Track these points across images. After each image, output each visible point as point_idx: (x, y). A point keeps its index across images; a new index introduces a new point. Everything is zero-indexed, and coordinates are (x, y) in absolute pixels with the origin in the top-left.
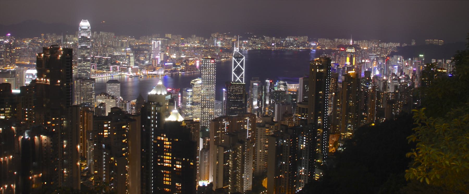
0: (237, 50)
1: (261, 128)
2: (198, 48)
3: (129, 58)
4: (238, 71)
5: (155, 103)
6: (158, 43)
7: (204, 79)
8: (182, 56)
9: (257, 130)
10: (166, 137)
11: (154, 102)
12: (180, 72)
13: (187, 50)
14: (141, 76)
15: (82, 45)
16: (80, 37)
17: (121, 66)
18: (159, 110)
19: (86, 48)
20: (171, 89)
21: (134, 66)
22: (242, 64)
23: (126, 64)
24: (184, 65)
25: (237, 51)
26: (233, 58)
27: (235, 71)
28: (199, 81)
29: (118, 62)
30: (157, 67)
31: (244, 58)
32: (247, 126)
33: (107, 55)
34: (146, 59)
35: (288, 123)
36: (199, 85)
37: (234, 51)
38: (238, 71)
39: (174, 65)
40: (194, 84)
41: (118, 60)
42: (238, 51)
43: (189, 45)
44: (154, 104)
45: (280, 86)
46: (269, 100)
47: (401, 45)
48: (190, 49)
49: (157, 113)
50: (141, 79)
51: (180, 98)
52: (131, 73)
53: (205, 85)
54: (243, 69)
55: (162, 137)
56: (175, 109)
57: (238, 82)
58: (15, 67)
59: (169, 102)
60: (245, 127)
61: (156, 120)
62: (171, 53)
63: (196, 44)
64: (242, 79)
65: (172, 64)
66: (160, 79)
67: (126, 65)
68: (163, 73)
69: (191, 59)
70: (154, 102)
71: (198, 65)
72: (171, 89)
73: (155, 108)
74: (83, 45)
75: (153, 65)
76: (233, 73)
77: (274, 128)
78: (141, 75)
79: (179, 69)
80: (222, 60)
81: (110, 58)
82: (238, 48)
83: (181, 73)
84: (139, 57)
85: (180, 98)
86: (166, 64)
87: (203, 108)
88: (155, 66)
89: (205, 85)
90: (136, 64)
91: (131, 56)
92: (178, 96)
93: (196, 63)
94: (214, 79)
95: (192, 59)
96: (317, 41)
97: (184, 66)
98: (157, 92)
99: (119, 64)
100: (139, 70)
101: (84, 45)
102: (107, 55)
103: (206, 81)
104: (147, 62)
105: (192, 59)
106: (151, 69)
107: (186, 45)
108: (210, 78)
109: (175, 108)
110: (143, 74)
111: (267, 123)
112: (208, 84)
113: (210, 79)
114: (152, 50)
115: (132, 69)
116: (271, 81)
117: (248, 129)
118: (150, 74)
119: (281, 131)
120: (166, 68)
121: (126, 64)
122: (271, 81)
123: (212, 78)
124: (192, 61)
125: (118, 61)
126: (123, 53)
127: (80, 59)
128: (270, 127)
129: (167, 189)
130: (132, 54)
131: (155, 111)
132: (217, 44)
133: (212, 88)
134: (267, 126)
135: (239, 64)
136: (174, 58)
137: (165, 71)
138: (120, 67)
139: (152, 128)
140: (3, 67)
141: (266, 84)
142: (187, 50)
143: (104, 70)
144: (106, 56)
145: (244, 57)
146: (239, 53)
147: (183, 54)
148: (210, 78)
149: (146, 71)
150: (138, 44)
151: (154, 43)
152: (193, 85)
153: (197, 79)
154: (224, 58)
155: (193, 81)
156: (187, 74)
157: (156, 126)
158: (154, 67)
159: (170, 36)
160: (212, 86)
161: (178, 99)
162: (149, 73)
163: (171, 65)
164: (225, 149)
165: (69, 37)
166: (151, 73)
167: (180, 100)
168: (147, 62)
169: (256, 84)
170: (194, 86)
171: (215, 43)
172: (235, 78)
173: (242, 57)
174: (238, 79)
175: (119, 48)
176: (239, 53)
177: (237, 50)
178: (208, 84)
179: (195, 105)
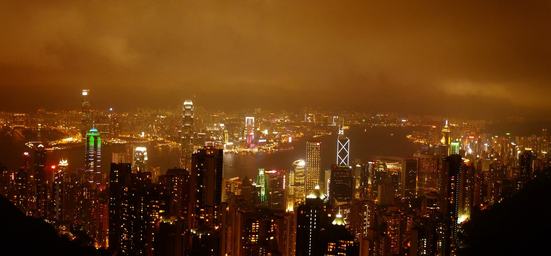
2: (287, 124)
3: (224, 135)
4: (343, 154)
6: (252, 119)
7: (309, 162)
8: (274, 132)
12: (274, 150)
13: (278, 126)
15: (186, 125)
17: (215, 142)
20: (276, 171)
21: (229, 142)
22: (346, 147)
23: (220, 140)
24: (278, 142)
25: (341, 133)
26: (338, 141)
28: (301, 163)
31: (349, 140)
33: (201, 131)
34: (239, 136)
36: (301, 166)
37: (339, 134)
38: (343, 154)
39: (267, 142)
40: (296, 166)
43: (279, 121)
48: (282, 124)
51: (284, 180)
52: (226, 150)
53: (310, 168)
54: (348, 151)
57: (343, 164)
58: (118, 140)
62: (262, 129)
63: (286, 119)
64: (346, 161)
65: (265, 141)
67: (220, 142)
69: (283, 136)
71: (290, 141)
72: (276, 171)
73: (313, 211)
75: (246, 142)
76: (338, 155)
80: (314, 137)
83: (274, 151)
84: (233, 133)
85: (284, 180)
86: (260, 141)
87: (308, 190)
88: (249, 143)
89: (310, 168)
90: (230, 141)
91: (225, 133)
92: (283, 178)
93: (288, 140)
94: (318, 162)
95: (285, 135)
97: (277, 143)
99: (213, 140)
100: (233, 147)
102: (201, 131)
103: (311, 163)
104: (240, 139)
105: (285, 135)
106: (245, 145)
107: (276, 121)
108: (316, 161)
109: (339, 213)
110: (237, 151)
112: (313, 167)
113: (316, 162)
114: (246, 126)
118: (245, 151)
120: (260, 146)
121: (220, 140)
123: (318, 161)
124: (284, 138)
127: (184, 138)
130: (227, 131)
132: (307, 120)
133: (317, 170)
135: (343, 147)
136: (266, 135)
137: (259, 148)
138: (215, 144)
139: (310, 228)
140: (109, 140)
142: (278, 126)
144: (200, 133)
145: (348, 140)
148: (316, 161)
149: (241, 148)
151: (248, 120)
153: (299, 161)
154: (317, 134)
155: (295, 162)
157: (315, 227)
159: (259, 110)
160: (317, 168)
161: (283, 181)
162: (243, 150)
163: (264, 142)
165: (162, 110)
166: (245, 150)
167: (284, 182)
168: (240, 139)
172: (340, 161)
177: (342, 133)
178: (313, 167)
179: (297, 186)
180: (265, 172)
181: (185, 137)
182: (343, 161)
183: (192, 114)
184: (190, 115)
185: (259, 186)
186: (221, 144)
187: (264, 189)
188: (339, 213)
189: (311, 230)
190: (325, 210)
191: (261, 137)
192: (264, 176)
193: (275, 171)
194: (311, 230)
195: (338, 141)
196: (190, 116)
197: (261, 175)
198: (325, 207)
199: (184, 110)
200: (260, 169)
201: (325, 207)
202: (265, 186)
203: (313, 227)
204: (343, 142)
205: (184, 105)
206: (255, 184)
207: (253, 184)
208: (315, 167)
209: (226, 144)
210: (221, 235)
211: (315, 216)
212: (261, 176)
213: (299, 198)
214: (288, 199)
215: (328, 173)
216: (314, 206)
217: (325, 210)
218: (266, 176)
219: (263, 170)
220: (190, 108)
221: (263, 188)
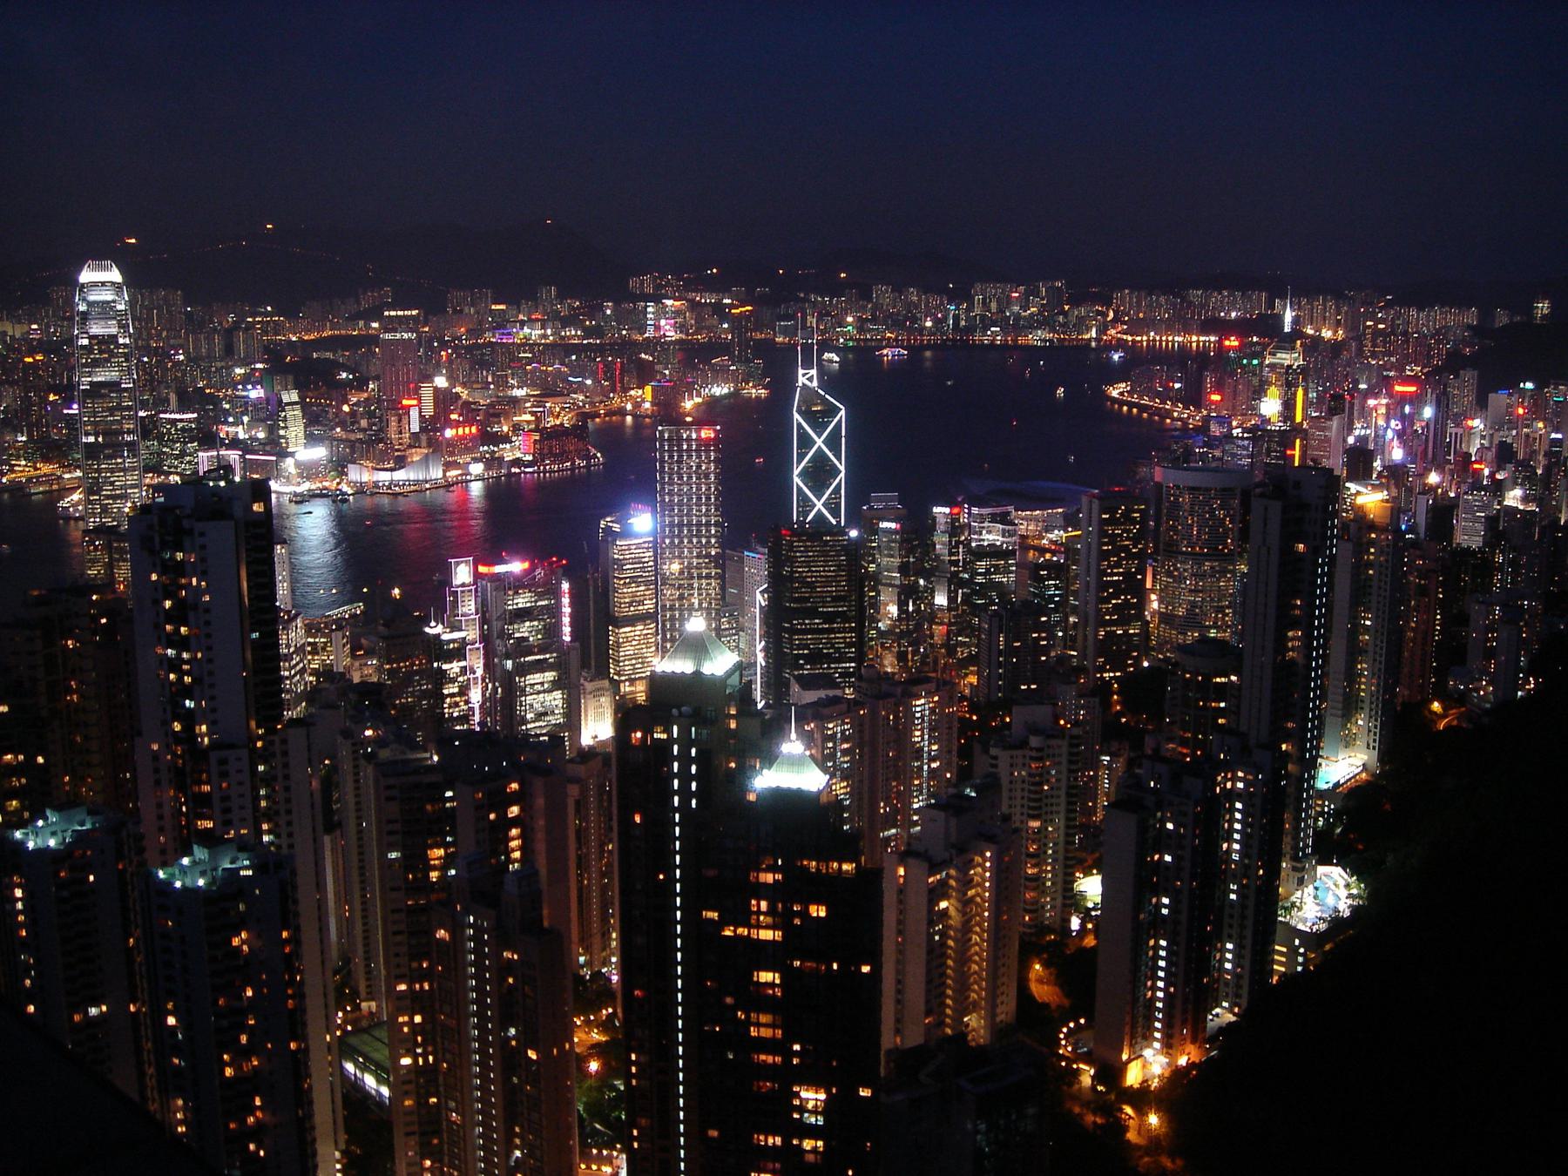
0: (810, 379)
1: (1015, 753)
5: (684, 709)
9: (994, 762)
11: (679, 708)
14: (346, 494)
16: (85, 342)
19: (114, 386)
20: (526, 565)
22: (832, 441)
26: (796, 416)
27: (804, 474)
29: (227, 433)
30: (410, 446)
32: (922, 736)
35: (1077, 707)
38: (819, 474)
41: (226, 423)
42: (815, 384)
44: (681, 714)
46: (949, 592)
47: (1486, 314)
48: (545, 352)
50: (345, 506)
54: (839, 459)
56: (791, 741)
59: (740, 700)
60: (916, 739)
61: (693, 778)
68: (440, 475)
70: (679, 708)
72: (526, 565)
74: (99, 379)
77: (1065, 750)
78: (345, 488)
79: (509, 457)
81: (195, 415)
82: (814, 372)
86: (449, 433)
90: (311, 439)
91: (288, 404)
96: (1109, 304)
98: (699, 664)
99: (235, 443)
101: (101, 377)
109: (793, 736)
110: (348, 483)
111: (1035, 730)
115: (298, 465)
117: (926, 749)
119: (1152, 784)
125: (226, 428)
126: (240, 387)
127: (91, 439)
129: (763, 1057)
131: (686, 743)
132: (657, 328)
134: (1034, 741)
135: (819, 442)
139: (676, 810)
141: (929, 526)
143: (171, 473)
146: (820, 391)
147: (514, 382)
150: (294, 339)
152: (610, 539)
156: (544, 472)
157: (694, 802)
158: (398, 450)
160: (708, 542)
164: (934, 868)
169: (893, 525)
170: (618, 543)
171: (649, 322)
172: (806, 504)
173: (833, 411)
174: (819, 514)
175: (219, 364)
176: (820, 391)
177: (810, 379)
180: (476, 569)
181: (96, 439)
182: (819, 505)
183: (123, 326)
184: (114, 331)
185: (456, 635)
186: (274, 458)
187: (478, 649)
188: (793, 736)
189: (677, 816)
190: (733, 725)
191: (454, 416)
192: (473, 588)
193: (523, 561)
194: (677, 816)
195: (796, 416)
196: (115, 337)
197: (463, 585)
198: (733, 712)
199: (82, 308)
200: (453, 561)
201: (733, 712)
202: (485, 638)
203: (685, 802)
204: (818, 420)
205: (83, 285)
206: (439, 629)
207: (427, 630)
208: (699, 536)
209: (292, 454)
210: (294, 873)
211: (693, 751)
212: (459, 589)
213: (636, 679)
214: (589, 686)
215: (756, 565)
217: (733, 725)
218: (484, 590)
219: (466, 562)
220: (109, 297)
221: (477, 645)
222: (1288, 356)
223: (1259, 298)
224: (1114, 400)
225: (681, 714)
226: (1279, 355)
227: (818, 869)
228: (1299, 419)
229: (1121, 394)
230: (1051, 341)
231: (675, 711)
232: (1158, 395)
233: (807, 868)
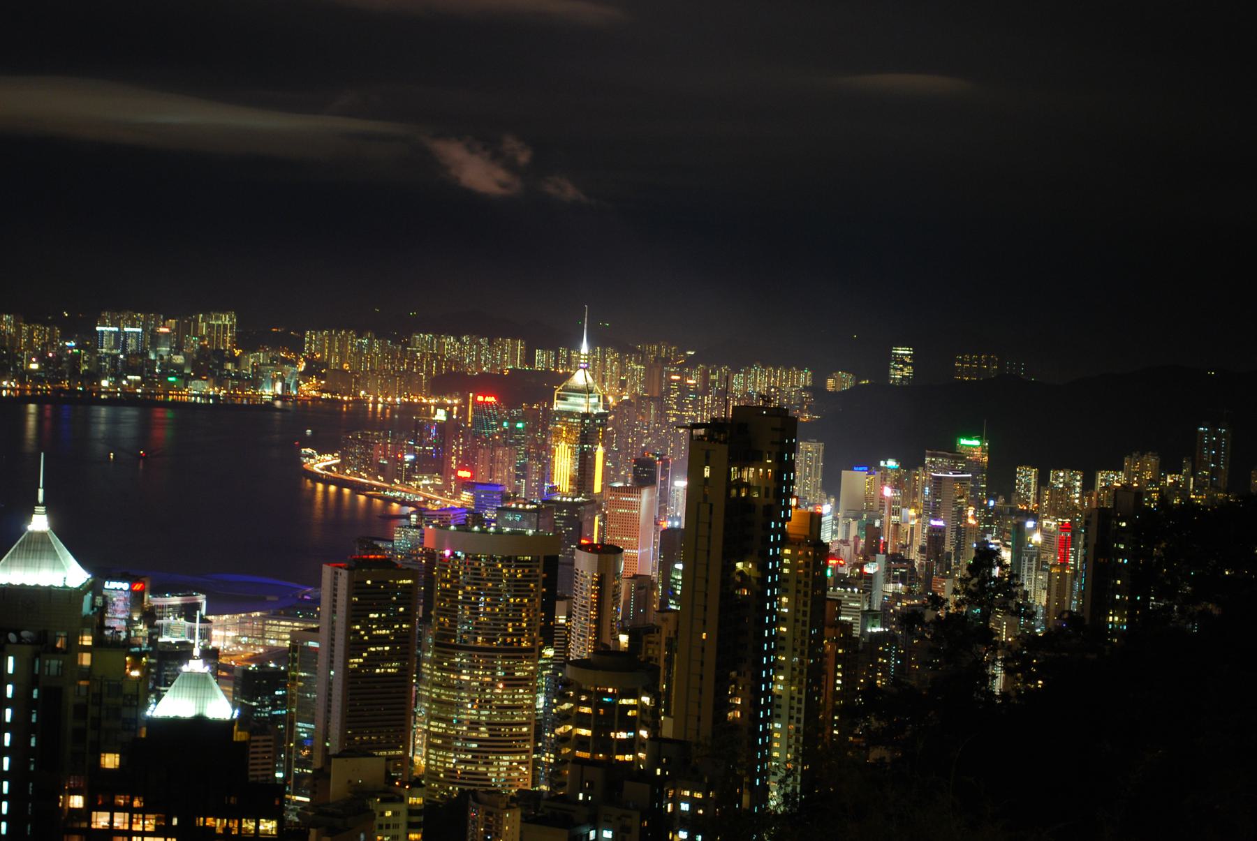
5: (24, 634)
10: (144, 811)
11: (17, 633)
18: (53, 670)
44: (20, 640)
45: (164, 621)
49: (35, 692)
55: (116, 814)
66: (41, 499)
77: (403, 819)
96: (297, 347)
116: (138, 587)
119: (581, 796)
122: (138, 587)
128: (383, 814)
216: (24, 634)
217: (86, 659)
222: (581, 401)
223: (514, 349)
224: (316, 478)
225: (20, 640)
226: (571, 400)
227: (227, 830)
228: (597, 488)
229: (328, 468)
230: (216, 397)
231: (12, 637)
232: (382, 470)
233: (213, 829)
